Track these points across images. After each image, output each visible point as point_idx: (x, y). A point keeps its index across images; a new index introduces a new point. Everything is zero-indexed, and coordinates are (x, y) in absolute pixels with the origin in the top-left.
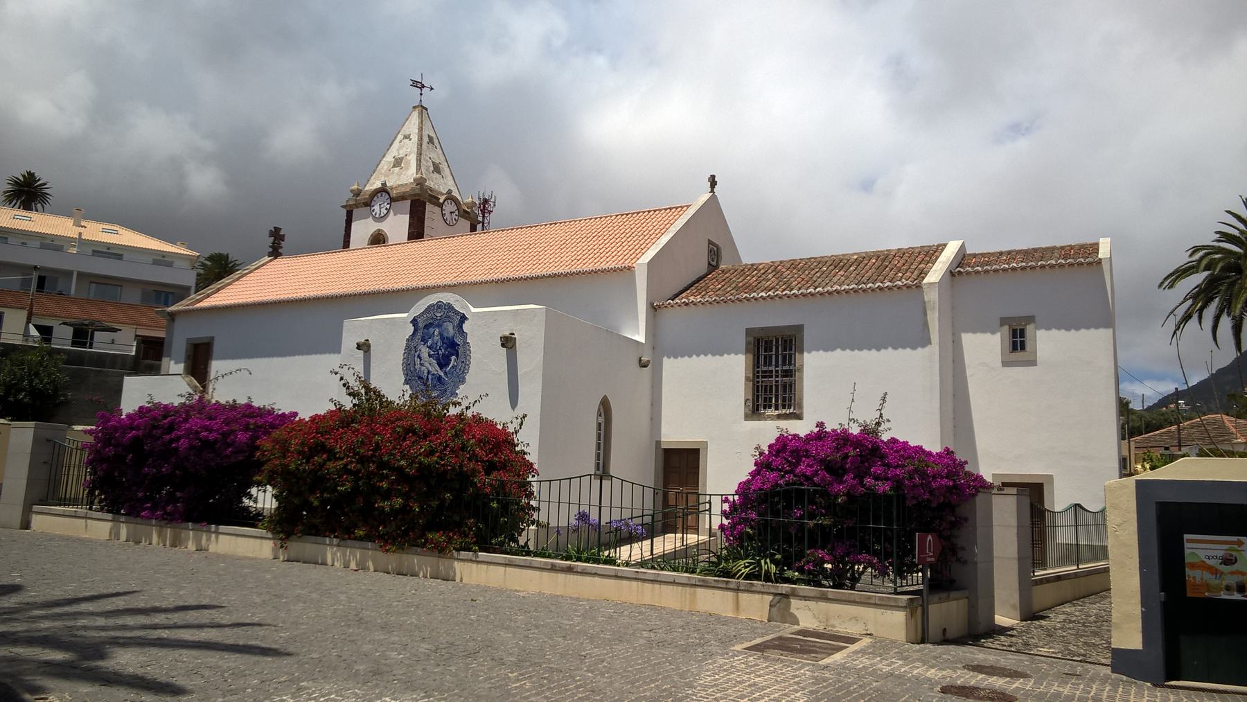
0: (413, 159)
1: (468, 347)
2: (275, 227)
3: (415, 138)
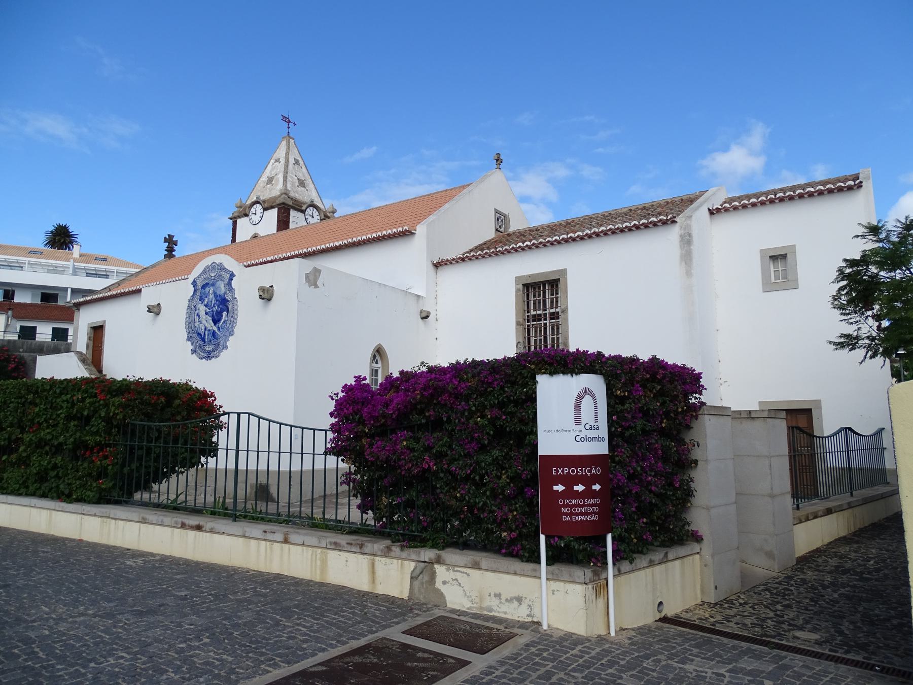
0: (280, 177)
2: (169, 235)
3: (283, 161)
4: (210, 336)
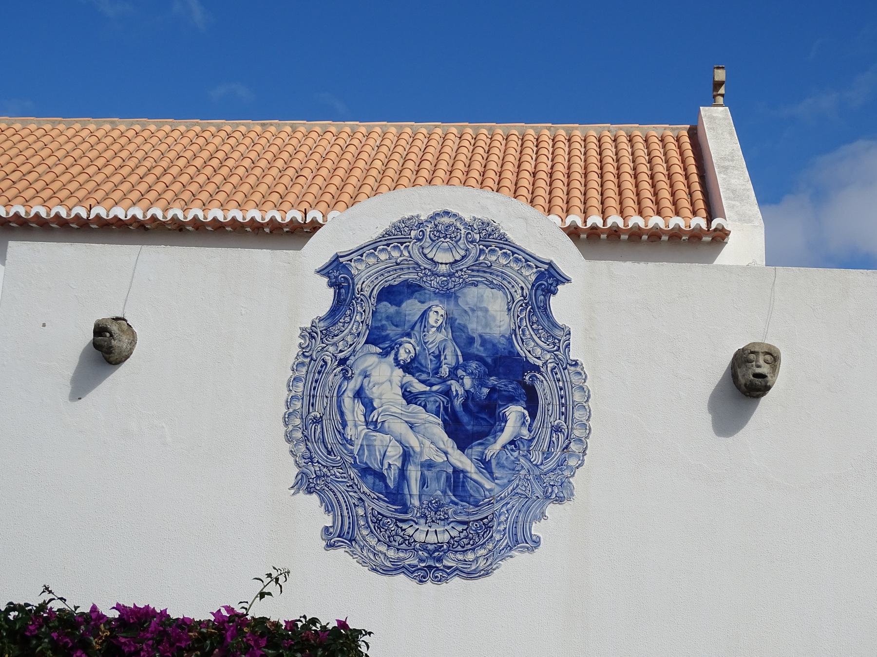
1: (575, 379)
4: (436, 489)
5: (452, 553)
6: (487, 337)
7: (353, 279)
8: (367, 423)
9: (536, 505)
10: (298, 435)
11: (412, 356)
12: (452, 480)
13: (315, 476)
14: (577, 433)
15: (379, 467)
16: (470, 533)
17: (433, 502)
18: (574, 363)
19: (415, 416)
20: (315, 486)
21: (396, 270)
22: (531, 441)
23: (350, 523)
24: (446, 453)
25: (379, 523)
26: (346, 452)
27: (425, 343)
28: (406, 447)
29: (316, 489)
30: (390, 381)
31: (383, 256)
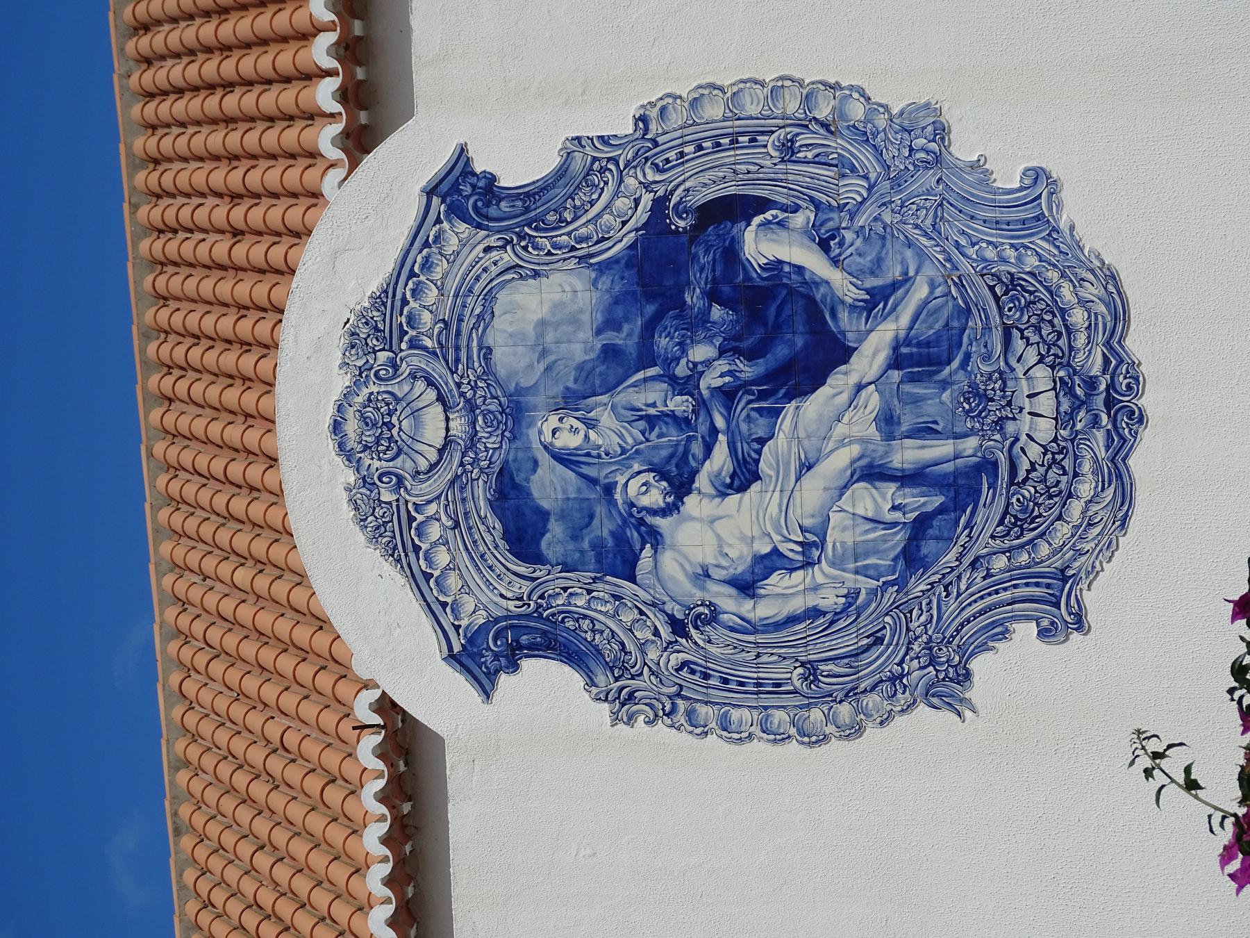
5: (1074, 358)
6: (600, 318)
7: (497, 620)
8: (808, 564)
9: (956, 184)
10: (845, 710)
11: (654, 477)
12: (917, 369)
13: (931, 668)
14: (792, 105)
15: (901, 529)
16: (1028, 321)
17: (967, 407)
18: (641, 125)
19: (783, 459)
20: (952, 667)
21: (470, 528)
22: (817, 205)
23: (1027, 585)
24: (860, 387)
25: (1021, 520)
26: (874, 605)
27: (624, 451)
28: (852, 476)
29: (960, 662)
30: (712, 521)
31: (442, 558)
